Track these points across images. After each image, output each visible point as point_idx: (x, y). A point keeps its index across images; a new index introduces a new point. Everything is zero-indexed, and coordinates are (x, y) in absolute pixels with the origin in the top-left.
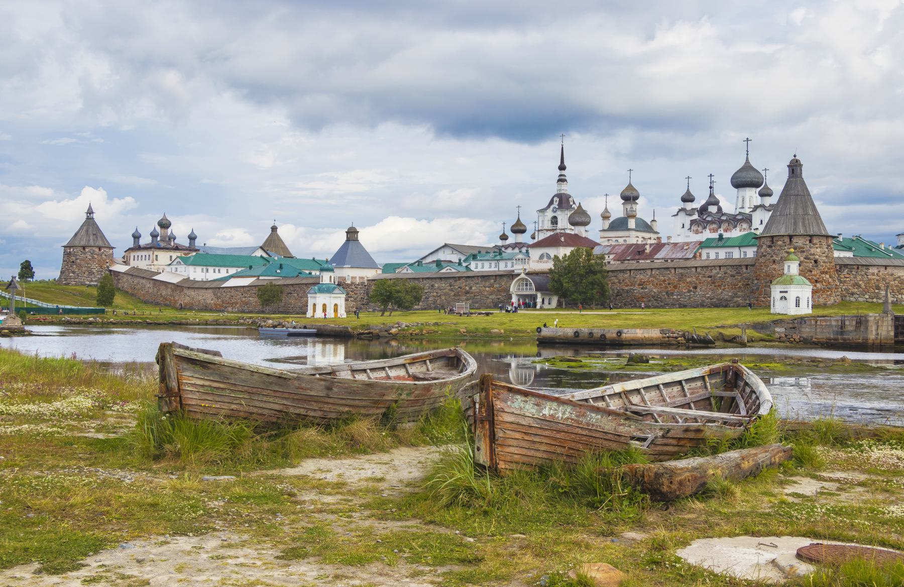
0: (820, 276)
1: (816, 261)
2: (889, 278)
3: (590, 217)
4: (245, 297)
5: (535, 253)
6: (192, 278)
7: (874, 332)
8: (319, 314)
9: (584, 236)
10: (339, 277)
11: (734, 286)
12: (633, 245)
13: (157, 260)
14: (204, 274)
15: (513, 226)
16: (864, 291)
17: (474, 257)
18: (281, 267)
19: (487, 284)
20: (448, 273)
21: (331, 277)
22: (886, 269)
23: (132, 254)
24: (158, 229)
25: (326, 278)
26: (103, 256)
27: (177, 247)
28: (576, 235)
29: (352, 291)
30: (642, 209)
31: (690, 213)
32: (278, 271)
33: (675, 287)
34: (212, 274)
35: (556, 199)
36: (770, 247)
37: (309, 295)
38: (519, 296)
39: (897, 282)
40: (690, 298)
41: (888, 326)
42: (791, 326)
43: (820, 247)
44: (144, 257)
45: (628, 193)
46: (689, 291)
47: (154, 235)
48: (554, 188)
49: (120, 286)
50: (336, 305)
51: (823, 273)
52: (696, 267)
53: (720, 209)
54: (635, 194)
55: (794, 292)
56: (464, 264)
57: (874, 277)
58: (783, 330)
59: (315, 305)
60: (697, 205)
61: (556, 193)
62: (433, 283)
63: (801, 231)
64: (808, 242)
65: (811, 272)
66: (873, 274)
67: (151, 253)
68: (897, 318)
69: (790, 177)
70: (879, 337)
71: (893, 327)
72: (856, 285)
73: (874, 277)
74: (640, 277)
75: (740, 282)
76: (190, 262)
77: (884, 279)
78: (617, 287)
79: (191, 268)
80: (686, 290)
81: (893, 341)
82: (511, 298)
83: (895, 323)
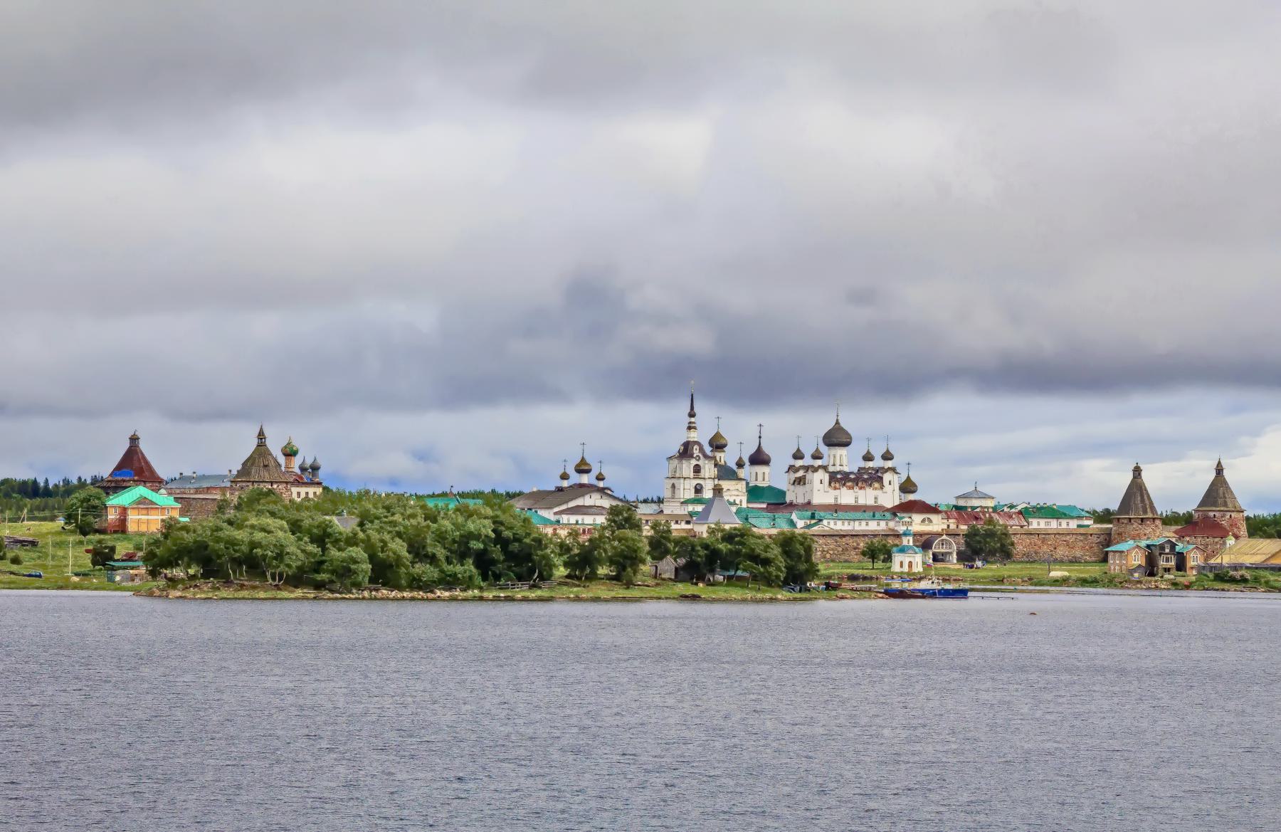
3: (916, 486)
11: (1083, 548)
15: (577, 466)
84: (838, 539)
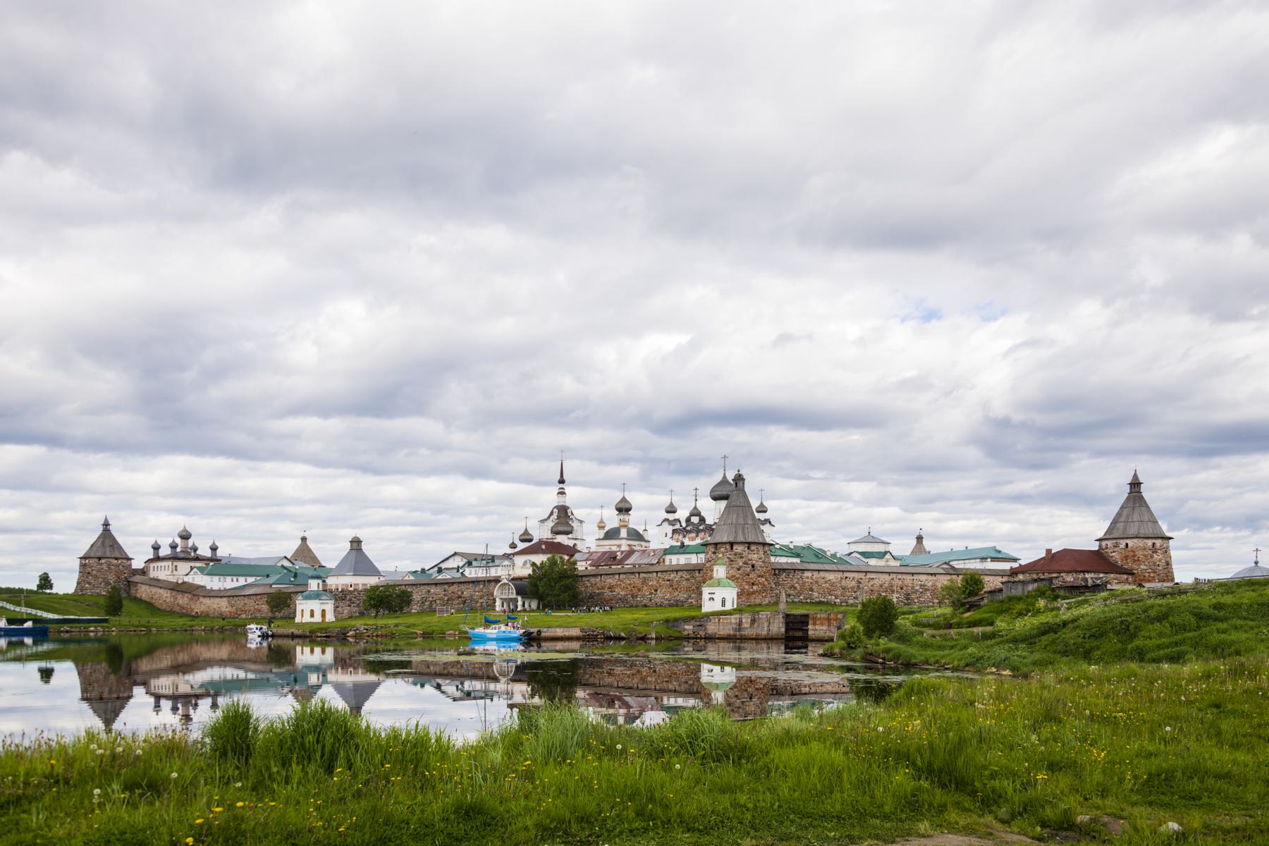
1: (753, 566)
2: (821, 581)
4: (258, 604)
5: (519, 560)
6: (208, 588)
7: (766, 629)
8: (307, 619)
9: (566, 544)
10: (342, 585)
12: (606, 552)
13: (176, 570)
14: (220, 583)
17: (470, 564)
18: (295, 576)
19: (477, 589)
20: (442, 579)
21: (318, 584)
23: (152, 565)
24: (178, 540)
25: (314, 585)
26: (121, 567)
27: (197, 557)
28: (559, 543)
29: (355, 598)
30: (635, 520)
31: (672, 523)
32: (292, 579)
33: (639, 590)
34: (229, 583)
35: (556, 510)
36: (714, 553)
37: (297, 602)
38: (503, 600)
40: (651, 600)
41: (779, 623)
42: (698, 623)
43: (757, 553)
44: (163, 567)
45: (623, 506)
46: (651, 594)
47: (174, 547)
49: (138, 596)
50: (323, 611)
51: (759, 576)
52: (657, 572)
53: (702, 520)
54: (627, 506)
55: (720, 593)
56: (461, 571)
57: (808, 580)
58: (691, 627)
59: (303, 610)
60: (682, 514)
61: (556, 505)
62: (429, 589)
63: (741, 539)
64: (746, 549)
65: (749, 575)
66: (808, 578)
67: (170, 563)
68: (787, 616)
70: (770, 633)
71: (784, 625)
72: (793, 587)
73: (808, 580)
74: (610, 581)
75: (694, 585)
76: (205, 573)
77: (817, 582)
78: (589, 590)
79: (208, 578)
81: (784, 637)
82: (494, 600)
83: (786, 620)
84: (446, 586)
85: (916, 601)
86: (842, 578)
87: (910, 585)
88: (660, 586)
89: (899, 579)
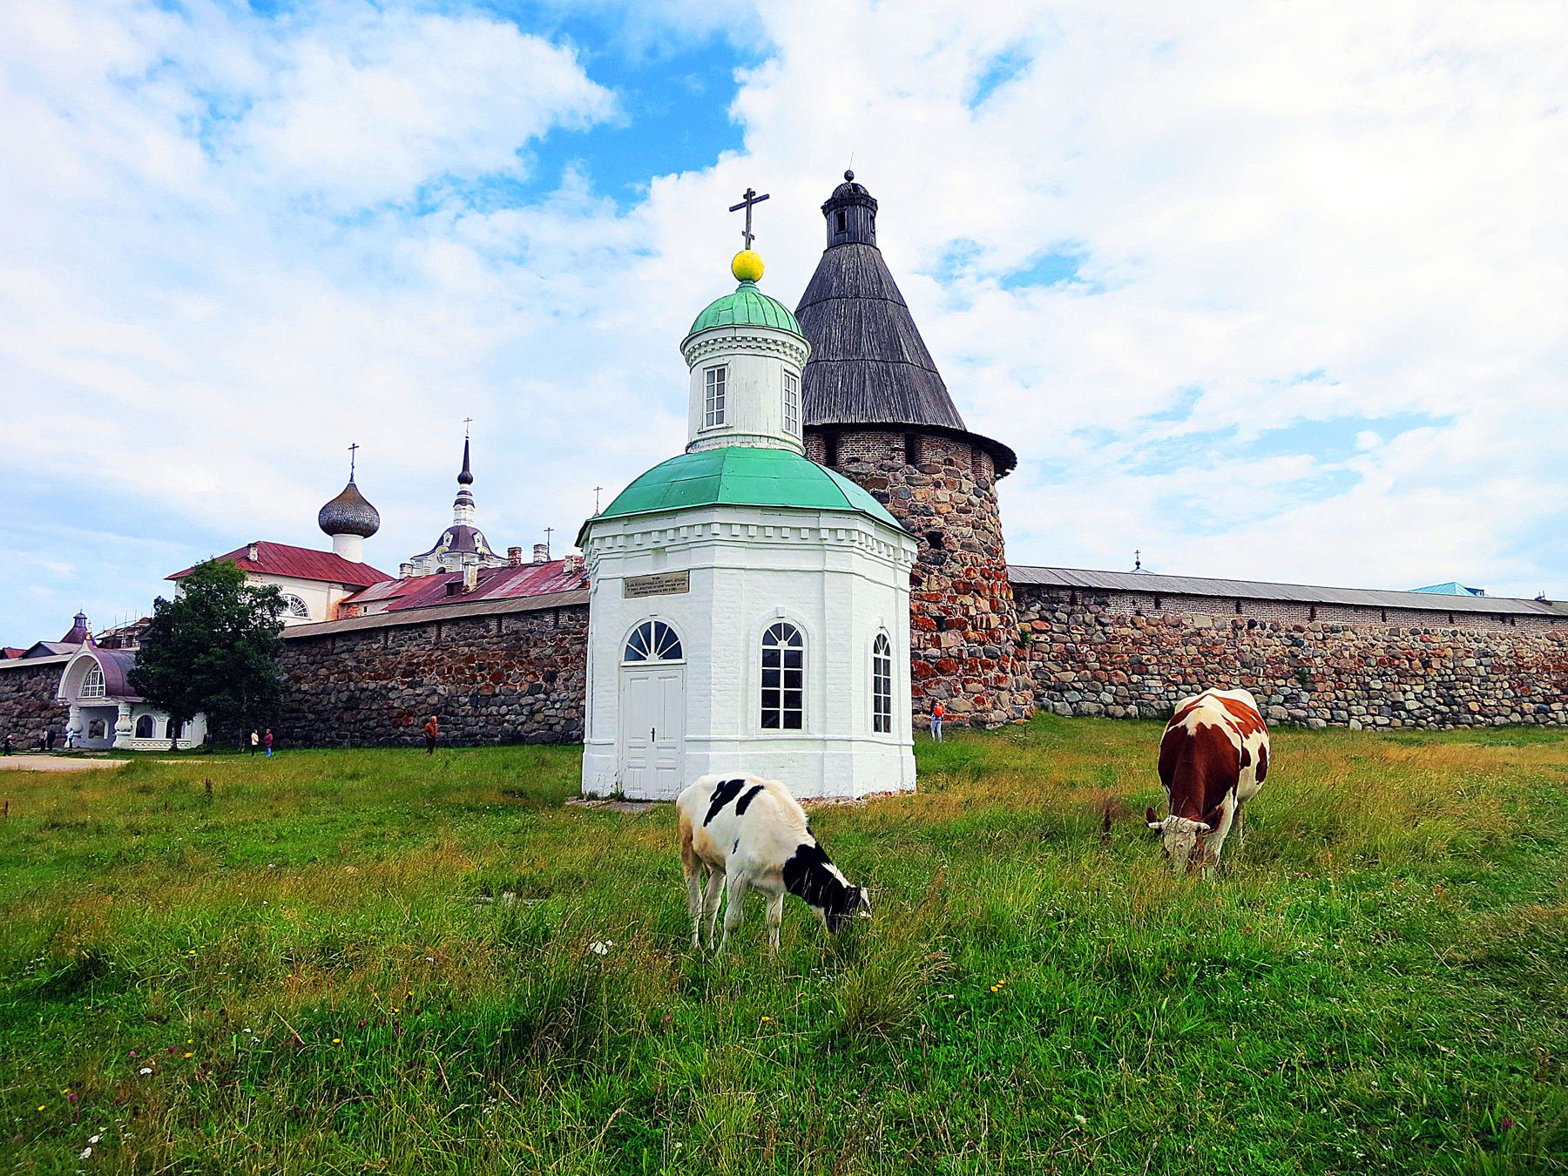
0: (952, 599)
16: (1095, 678)
22: (1158, 605)
33: (497, 678)
39: (1193, 649)
40: (532, 713)
48: (447, 518)
51: (966, 588)
57: (1125, 631)
64: (900, 460)
69: (832, 246)
73: (1125, 631)
77: (1155, 640)
80: (526, 686)
85: (1474, 706)
86: (1236, 627)
87: (1450, 652)
88: (566, 661)
89: (1414, 632)
